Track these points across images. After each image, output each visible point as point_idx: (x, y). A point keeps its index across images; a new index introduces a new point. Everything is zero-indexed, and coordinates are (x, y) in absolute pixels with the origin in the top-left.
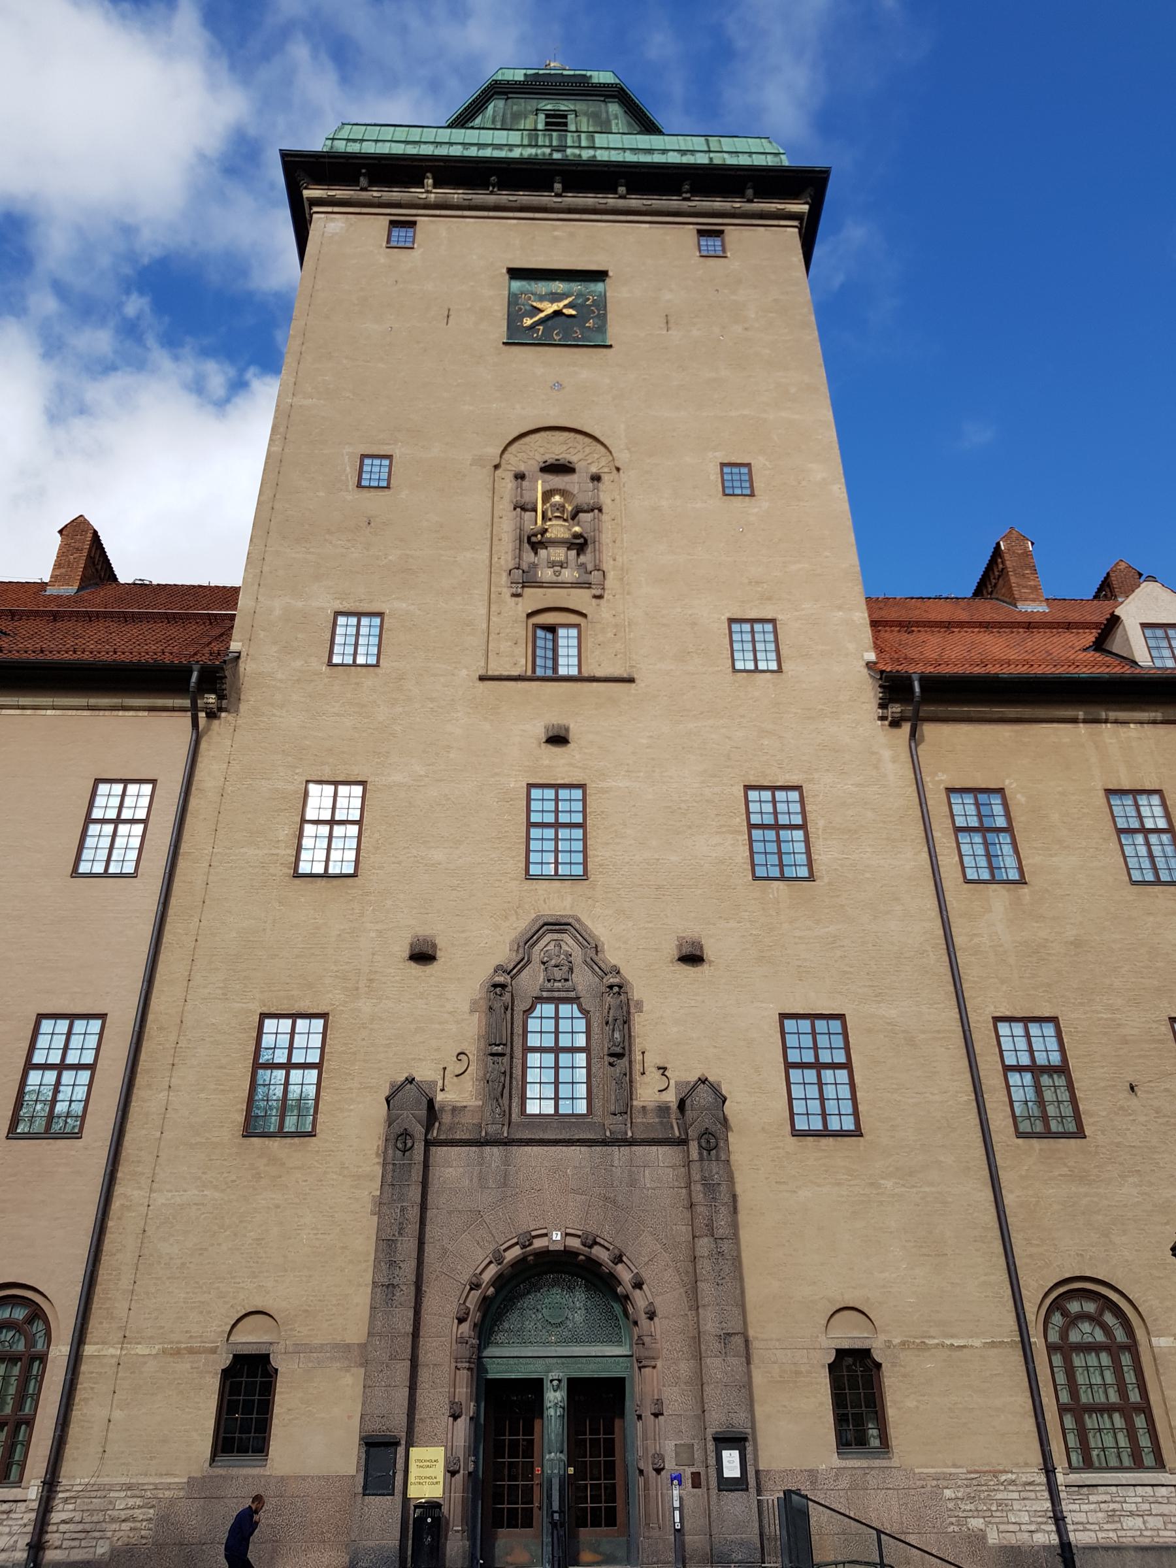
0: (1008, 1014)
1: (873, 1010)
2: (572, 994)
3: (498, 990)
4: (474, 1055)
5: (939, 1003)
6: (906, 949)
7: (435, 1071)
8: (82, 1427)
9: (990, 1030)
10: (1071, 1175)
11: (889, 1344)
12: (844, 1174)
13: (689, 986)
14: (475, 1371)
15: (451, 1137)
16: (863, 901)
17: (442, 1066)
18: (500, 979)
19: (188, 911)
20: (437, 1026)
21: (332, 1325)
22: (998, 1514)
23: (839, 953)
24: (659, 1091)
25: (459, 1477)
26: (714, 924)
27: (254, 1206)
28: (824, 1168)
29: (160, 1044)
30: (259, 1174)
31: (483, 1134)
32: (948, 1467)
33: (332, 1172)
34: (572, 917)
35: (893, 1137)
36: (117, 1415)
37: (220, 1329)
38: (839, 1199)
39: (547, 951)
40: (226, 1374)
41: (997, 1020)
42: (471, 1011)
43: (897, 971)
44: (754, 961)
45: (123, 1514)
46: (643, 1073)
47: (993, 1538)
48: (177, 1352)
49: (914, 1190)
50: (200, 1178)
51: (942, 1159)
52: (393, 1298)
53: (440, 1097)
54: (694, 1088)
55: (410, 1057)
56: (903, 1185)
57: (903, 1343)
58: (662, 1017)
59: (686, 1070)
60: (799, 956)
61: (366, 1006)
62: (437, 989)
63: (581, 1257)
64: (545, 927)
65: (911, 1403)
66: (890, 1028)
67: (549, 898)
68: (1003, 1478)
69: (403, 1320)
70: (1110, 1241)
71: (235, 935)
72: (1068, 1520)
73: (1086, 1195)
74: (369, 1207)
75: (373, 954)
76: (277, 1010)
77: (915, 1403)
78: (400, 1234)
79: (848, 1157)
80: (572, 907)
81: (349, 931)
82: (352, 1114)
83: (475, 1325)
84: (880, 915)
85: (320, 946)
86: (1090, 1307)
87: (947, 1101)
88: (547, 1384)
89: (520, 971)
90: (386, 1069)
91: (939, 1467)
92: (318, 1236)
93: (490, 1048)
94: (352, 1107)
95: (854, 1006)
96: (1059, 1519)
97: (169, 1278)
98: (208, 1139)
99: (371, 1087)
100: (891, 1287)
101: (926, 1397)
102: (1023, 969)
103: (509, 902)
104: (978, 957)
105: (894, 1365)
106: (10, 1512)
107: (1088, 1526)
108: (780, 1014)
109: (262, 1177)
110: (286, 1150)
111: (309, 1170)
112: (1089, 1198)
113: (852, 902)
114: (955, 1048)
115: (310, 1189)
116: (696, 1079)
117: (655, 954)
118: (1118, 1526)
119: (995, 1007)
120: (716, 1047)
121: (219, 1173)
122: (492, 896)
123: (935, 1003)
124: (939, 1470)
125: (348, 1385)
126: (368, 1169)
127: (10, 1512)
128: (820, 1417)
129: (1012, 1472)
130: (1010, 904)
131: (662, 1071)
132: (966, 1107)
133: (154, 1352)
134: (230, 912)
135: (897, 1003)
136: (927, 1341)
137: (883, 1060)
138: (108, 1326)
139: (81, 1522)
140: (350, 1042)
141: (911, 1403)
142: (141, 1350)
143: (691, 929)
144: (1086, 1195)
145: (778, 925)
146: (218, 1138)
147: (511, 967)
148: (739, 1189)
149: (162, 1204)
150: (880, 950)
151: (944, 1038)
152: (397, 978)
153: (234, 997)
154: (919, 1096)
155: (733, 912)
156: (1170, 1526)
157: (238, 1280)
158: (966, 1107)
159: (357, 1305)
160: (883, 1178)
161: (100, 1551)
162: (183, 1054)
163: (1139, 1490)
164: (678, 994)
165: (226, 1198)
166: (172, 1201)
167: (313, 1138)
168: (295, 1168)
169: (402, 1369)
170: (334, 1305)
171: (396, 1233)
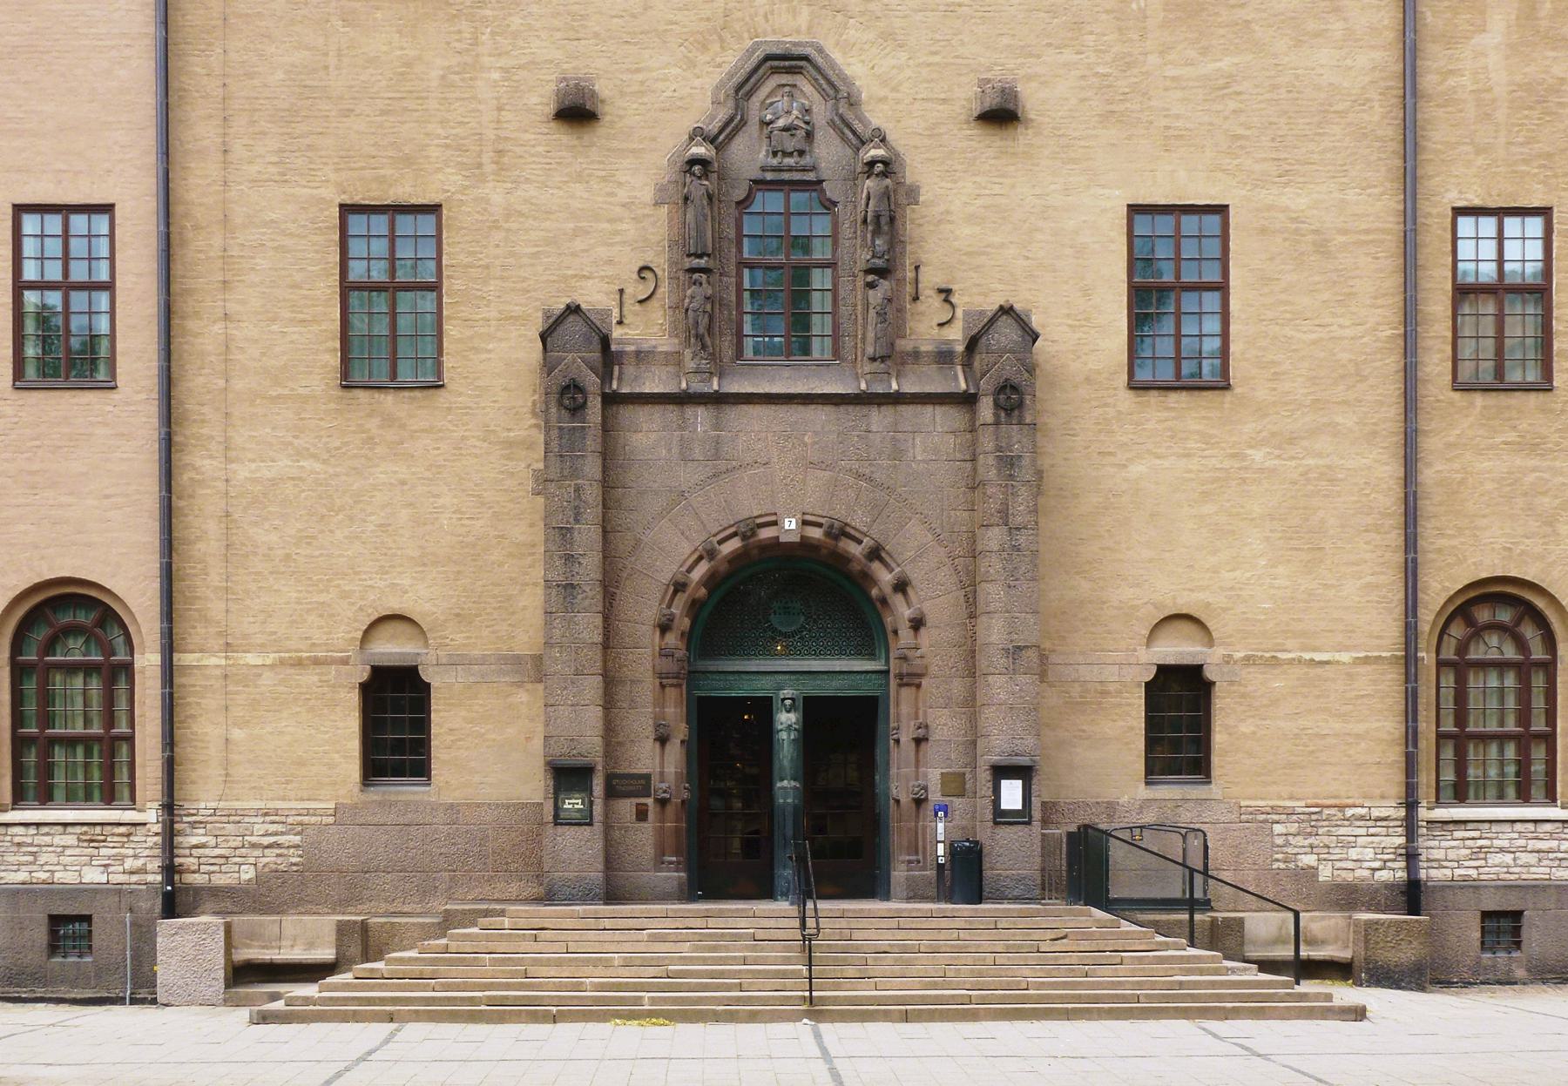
0: (1477, 202)
1: (1272, 197)
2: (811, 176)
3: (697, 168)
4: (664, 270)
5: (1375, 186)
6: (1338, 97)
7: (607, 294)
8: (195, 747)
9: (1445, 230)
10: (1519, 443)
11: (1228, 660)
12: (1196, 443)
13: (993, 162)
14: (684, 687)
15: (637, 390)
16: (1283, 14)
17: (617, 288)
18: (700, 150)
19: (203, 35)
20: (606, 225)
21: (493, 632)
22: (1337, 850)
23: (1232, 105)
24: (941, 325)
25: (670, 809)
26: (1039, 57)
27: (371, 481)
28: (1169, 434)
29: (200, 251)
30: (372, 438)
31: (684, 385)
32: (1284, 799)
33: (473, 437)
34: (812, 44)
35: (1275, 389)
36: (237, 734)
37: (350, 636)
38: (1185, 475)
39: (772, 104)
40: (365, 688)
41: (1459, 212)
42: (656, 204)
43: (1319, 134)
44: (1096, 118)
45: (267, 841)
46: (916, 298)
47: (1325, 874)
48: (299, 663)
49: (1293, 463)
50: (291, 444)
51: (1339, 419)
52: (574, 601)
53: (617, 333)
54: (992, 321)
55: (570, 272)
56: (1279, 457)
57: (1247, 658)
58: (948, 212)
59: (980, 294)
60: (1168, 110)
61: (495, 194)
62: (602, 166)
63: (824, 551)
64: (769, 63)
65: (1245, 728)
66: (1294, 226)
67: (772, 13)
68: (1349, 812)
69: (589, 626)
70: (1554, 531)
71: (282, 76)
72: (1423, 858)
73: (1534, 470)
74: (530, 485)
75: (500, 109)
76: (363, 199)
77: (1252, 728)
78: (577, 521)
79: (1204, 418)
80: (810, 28)
81: (457, 69)
82: (492, 356)
83: (683, 634)
84: (1306, 38)
85: (415, 95)
86: (1505, 616)
87: (1363, 337)
88: (776, 704)
89: (730, 138)
90: (535, 290)
91: (1271, 799)
92: (463, 522)
93: (686, 260)
94: (491, 346)
95: (1244, 192)
96: (1411, 857)
97: (271, 573)
98: (292, 390)
99: (516, 318)
100: (1241, 589)
101: (1268, 722)
102: (1516, 129)
103: (708, 19)
104: (1450, 109)
105: (1232, 683)
106: (129, 835)
107: (1445, 864)
108: (1129, 206)
109: (376, 444)
110: (406, 406)
111: (440, 434)
112: (1538, 474)
113: (1265, 15)
114: (1386, 257)
115: (445, 460)
116: (996, 307)
117: (941, 108)
118: (1482, 863)
119: (1460, 192)
120: (1028, 258)
121: (316, 437)
122: (680, 9)
123: (1369, 187)
124: (1271, 803)
125: (522, 703)
126: (523, 433)
127: (129, 835)
128: (1127, 744)
129: (1363, 807)
130: (1518, 18)
131: (943, 296)
132: (1388, 346)
133: (268, 662)
134: (268, 37)
135: (1312, 186)
136: (1279, 655)
137: (1276, 276)
138: (204, 631)
139: (216, 847)
140: (478, 249)
141: (1245, 728)
142: (252, 659)
143: (1003, 65)
144: (1534, 470)
145: (1141, 58)
146: (309, 389)
147: (716, 131)
148: (1045, 462)
149: (246, 478)
150: (1297, 99)
151: (1372, 241)
152: (540, 149)
153: (297, 178)
154: (1320, 329)
155: (1070, 35)
156: (1545, 862)
157: (364, 577)
158: (1388, 346)
159: (525, 608)
160: (1251, 447)
161: (245, 877)
162: (236, 266)
163: (1518, 826)
164: (974, 175)
165: (331, 471)
166: (258, 475)
167: (442, 390)
168: (422, 431)
169: (592, 686)
170: (495, 609)
171: (571, 520)
